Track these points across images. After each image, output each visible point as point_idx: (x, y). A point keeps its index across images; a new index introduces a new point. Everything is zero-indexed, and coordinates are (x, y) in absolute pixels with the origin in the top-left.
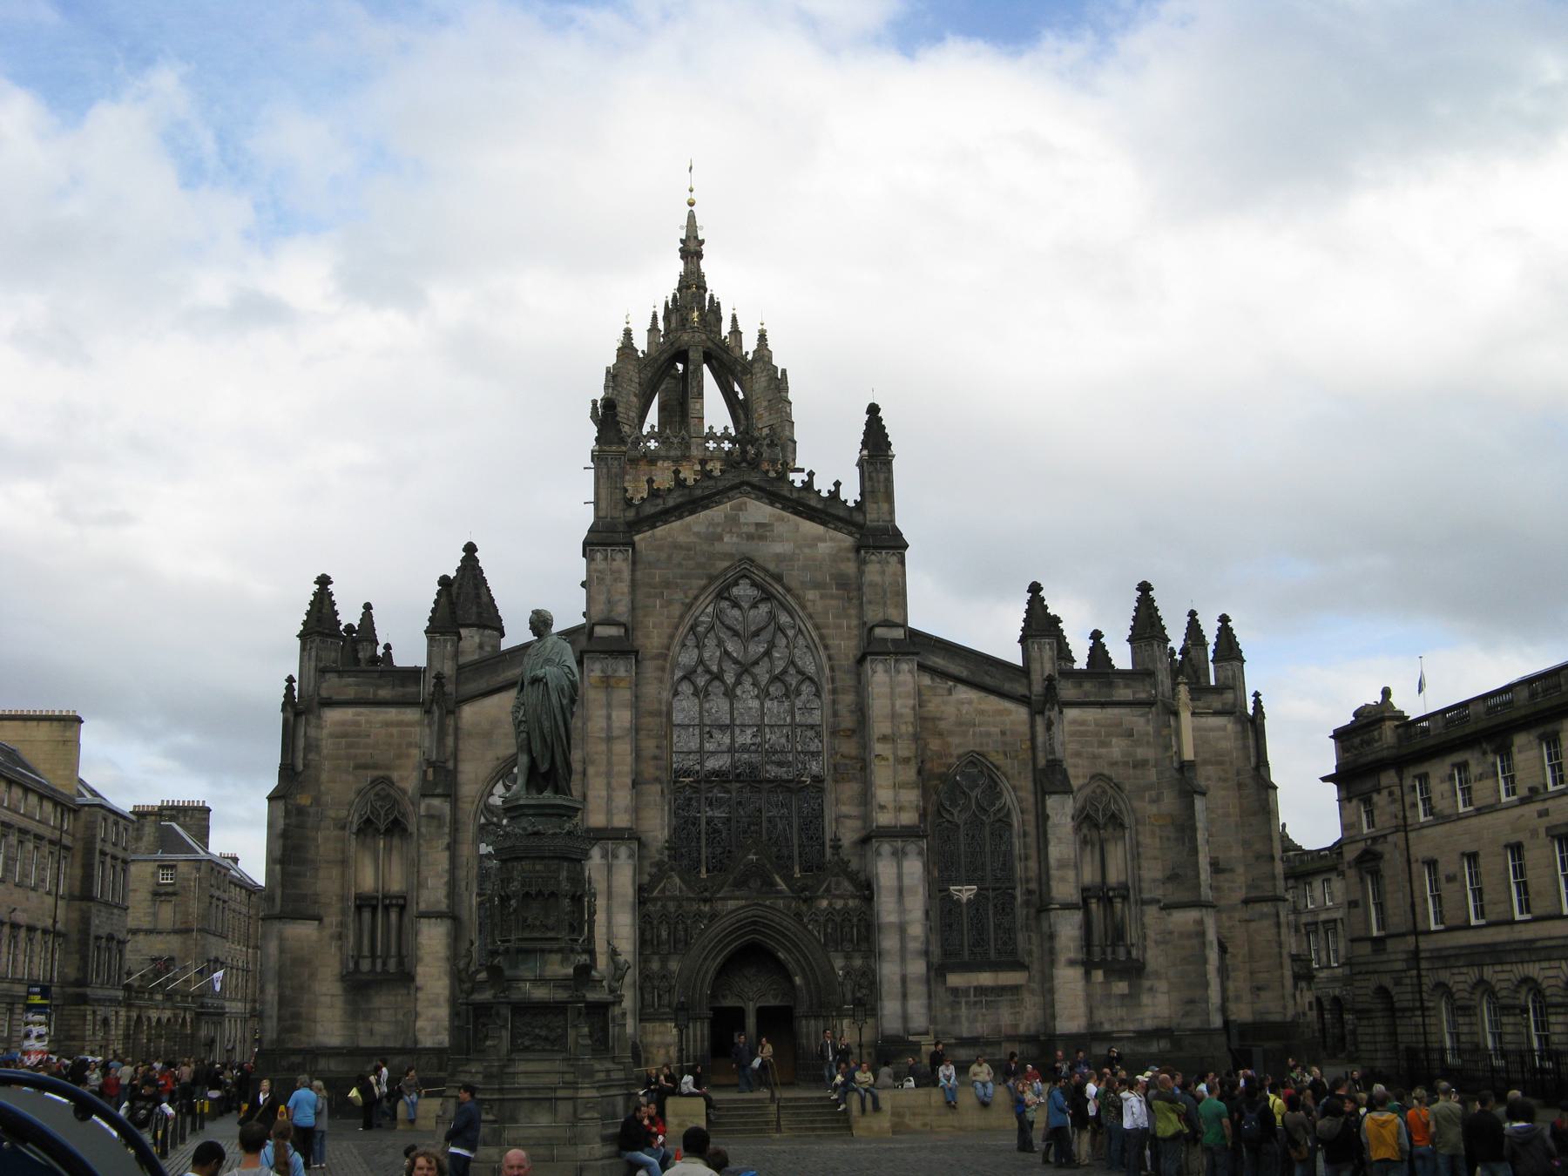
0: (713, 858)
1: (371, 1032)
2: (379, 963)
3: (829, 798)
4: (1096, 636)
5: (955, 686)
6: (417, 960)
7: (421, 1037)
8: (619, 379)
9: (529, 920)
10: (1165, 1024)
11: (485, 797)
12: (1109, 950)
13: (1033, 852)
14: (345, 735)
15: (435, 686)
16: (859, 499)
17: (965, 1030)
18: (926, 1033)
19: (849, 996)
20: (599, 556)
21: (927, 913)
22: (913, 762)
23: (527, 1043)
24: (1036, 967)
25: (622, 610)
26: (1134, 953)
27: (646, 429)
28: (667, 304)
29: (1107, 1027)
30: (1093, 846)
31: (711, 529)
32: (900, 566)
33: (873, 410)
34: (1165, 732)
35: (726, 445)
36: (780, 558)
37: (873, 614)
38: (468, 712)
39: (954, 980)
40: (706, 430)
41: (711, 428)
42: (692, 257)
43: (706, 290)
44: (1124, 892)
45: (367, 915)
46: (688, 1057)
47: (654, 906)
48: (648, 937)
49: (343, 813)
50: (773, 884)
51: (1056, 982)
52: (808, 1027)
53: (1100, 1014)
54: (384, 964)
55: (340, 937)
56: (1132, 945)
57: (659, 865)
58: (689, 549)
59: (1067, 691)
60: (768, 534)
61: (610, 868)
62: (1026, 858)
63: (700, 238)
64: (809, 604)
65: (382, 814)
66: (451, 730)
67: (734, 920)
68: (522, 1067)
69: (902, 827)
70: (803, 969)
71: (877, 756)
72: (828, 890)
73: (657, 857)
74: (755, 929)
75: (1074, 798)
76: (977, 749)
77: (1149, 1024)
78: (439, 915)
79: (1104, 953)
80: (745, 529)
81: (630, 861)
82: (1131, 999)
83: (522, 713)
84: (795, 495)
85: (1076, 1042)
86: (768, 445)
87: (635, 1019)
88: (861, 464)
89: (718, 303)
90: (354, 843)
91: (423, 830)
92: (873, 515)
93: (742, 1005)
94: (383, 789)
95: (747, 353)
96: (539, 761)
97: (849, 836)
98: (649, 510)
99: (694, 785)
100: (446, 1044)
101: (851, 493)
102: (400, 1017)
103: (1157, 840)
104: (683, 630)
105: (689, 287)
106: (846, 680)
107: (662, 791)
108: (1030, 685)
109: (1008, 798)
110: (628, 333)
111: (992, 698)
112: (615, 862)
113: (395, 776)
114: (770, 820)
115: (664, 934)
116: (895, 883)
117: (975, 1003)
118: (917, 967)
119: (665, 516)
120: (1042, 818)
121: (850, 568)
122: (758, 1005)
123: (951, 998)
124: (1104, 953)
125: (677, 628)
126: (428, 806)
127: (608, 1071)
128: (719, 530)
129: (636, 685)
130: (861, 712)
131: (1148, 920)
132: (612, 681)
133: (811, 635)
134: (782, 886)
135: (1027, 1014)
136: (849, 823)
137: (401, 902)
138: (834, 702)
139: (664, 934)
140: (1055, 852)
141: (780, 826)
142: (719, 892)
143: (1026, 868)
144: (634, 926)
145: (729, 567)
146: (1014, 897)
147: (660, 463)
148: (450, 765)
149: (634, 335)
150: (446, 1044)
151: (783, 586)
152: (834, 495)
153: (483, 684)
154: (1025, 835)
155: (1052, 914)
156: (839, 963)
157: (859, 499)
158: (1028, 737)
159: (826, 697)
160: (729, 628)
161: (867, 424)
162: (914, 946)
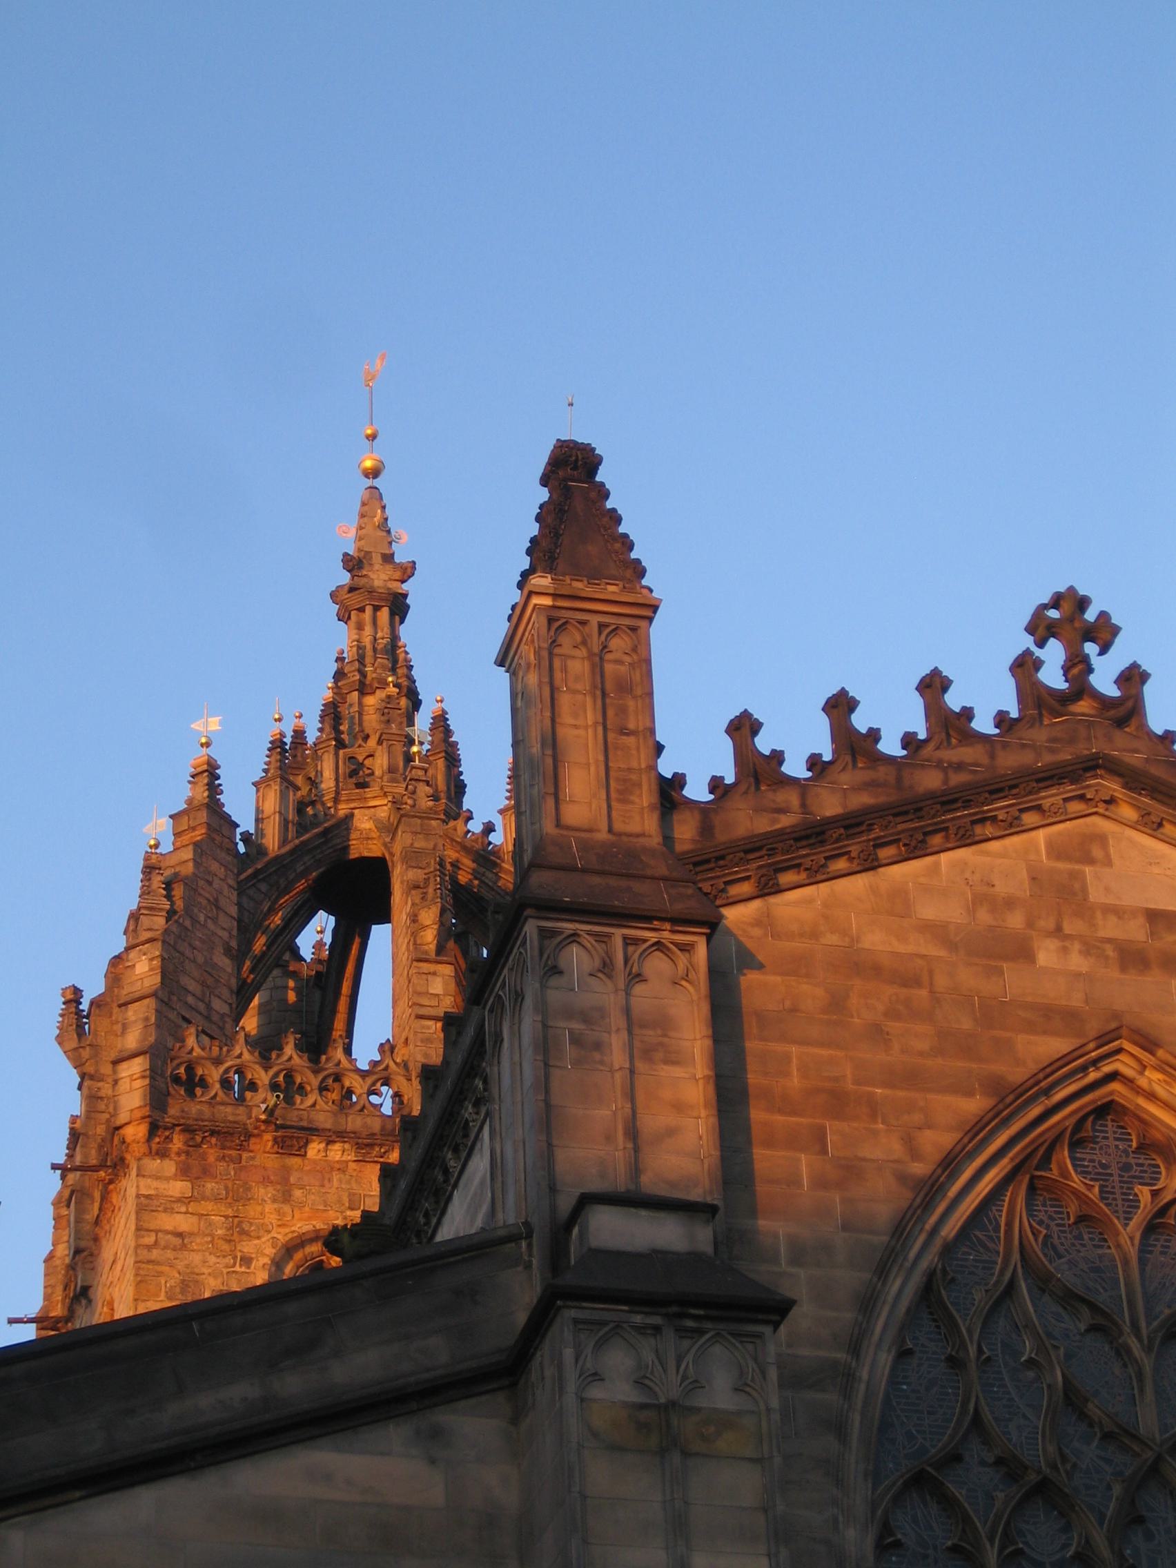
20: (577, 959)
31: (984, 916)
42: (376, 608)
58: (911, 981)
80: (1110, 928)
125: (882, 1271)
128: (1015, 921)
145: (1066, 1059)
147: (315, 1149)
149: (226, 779)
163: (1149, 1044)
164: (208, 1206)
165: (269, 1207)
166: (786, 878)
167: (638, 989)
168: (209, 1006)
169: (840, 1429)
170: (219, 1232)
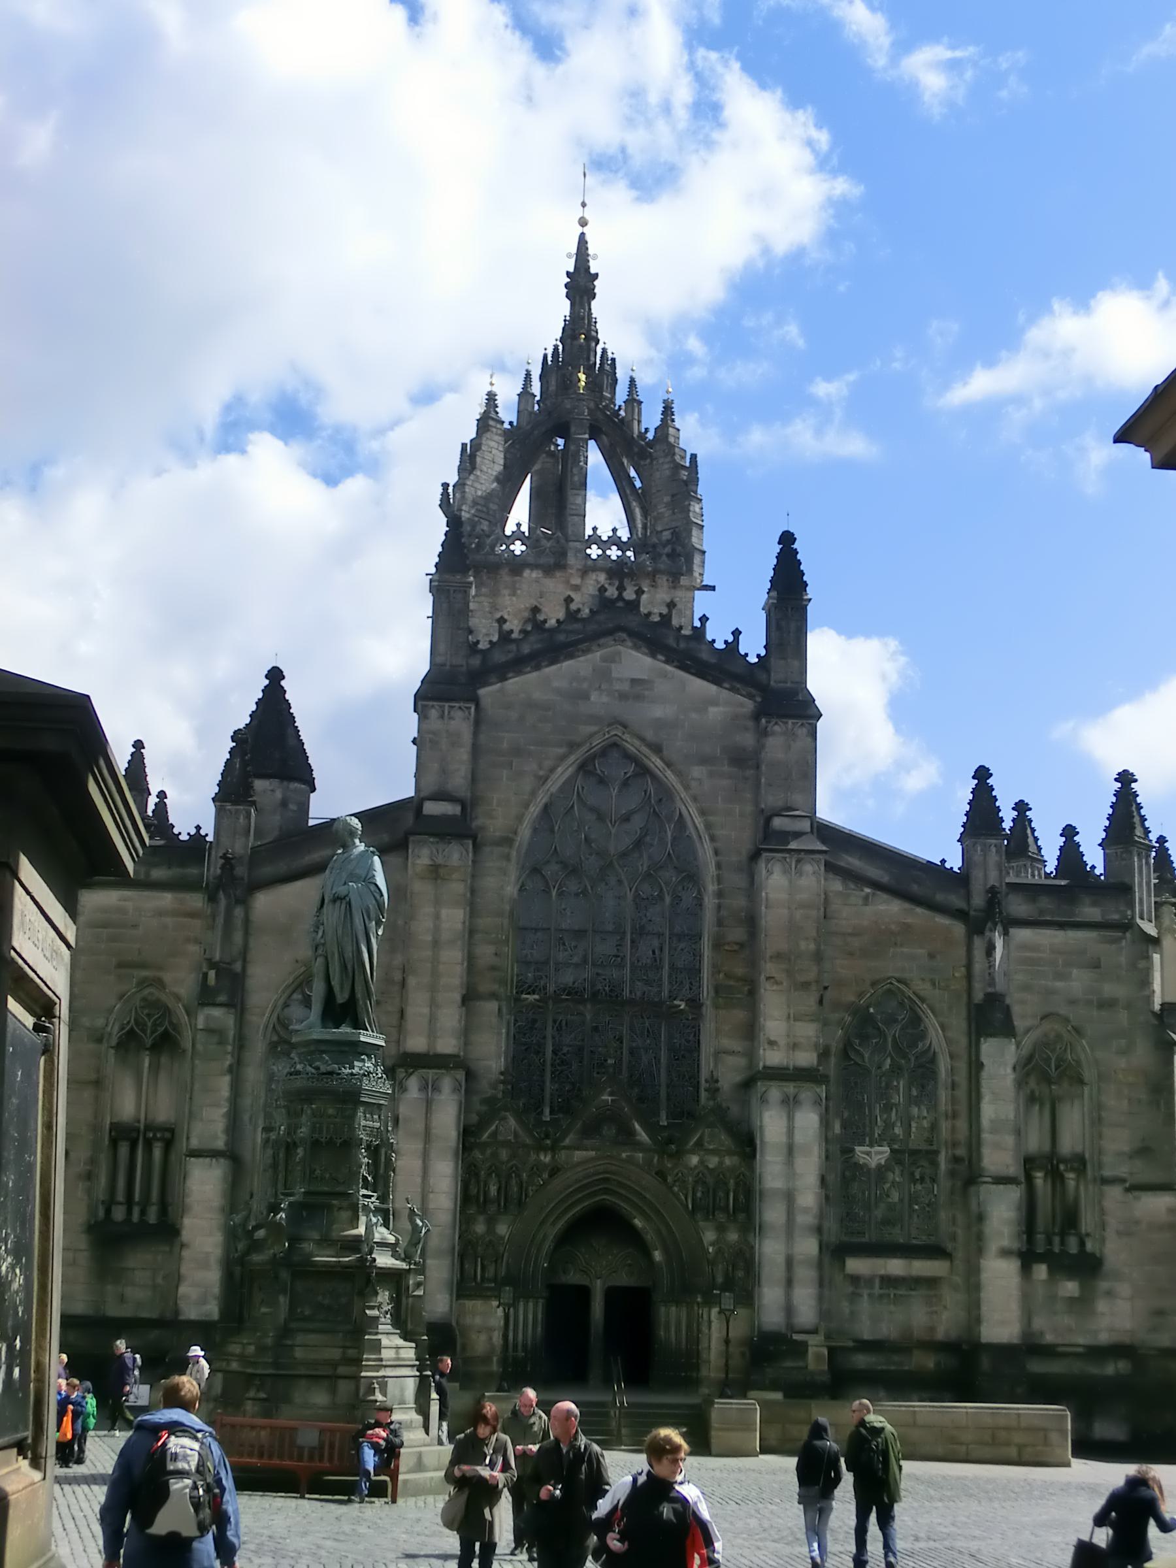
0: (559, 1096)
1: (122, 1299)
2: (136, 1211)
3: (708, 1027)
4: (1069, 832)
5: (874, 894)
6: (183, 1210)
7: (182, 1305)
8: (478, 460)
9: (318, 1172)
10: (1127, 1340)
11: (279, 1009)
12: (1057, 1240)
13: (963, 1108)
14: (105, 925)
15: (223, 867)
16: (763, 653)
17: (866, 1330)
18: (814, 1331)
20: (434, 713)
21: (823, 1180)
22: (814, 987)
23: (307, 1313)
24: (959, 1255)
25: (458, 781)
26: (1089, 1246)
27: (510, 529)
28: (545, 357)
29: (1049, 1338)
30: (1042, 1105)
32: (809, 739)
33: (787, 539)
34: (1142, 964)
35: (614, 553)
36: (659, 724)
37: (771, 799)
38: (264, 902)
39: (856, 1265)
40: (589, 532)
41: (595, 529)
42: (581, 297)
43: (597, 342)
44: (1079, 1163)
45: (124, 1149)
46: (515, 1346)
47: (483, 1153)
48: (473, 1191)
49: (100, 1022)
50: (631, 1133)
51: (985, 1276)
53: (1039, 1323)
54: (143, 1212)
55: (89, 1176)
56: (1088, 1235)
57: (490, 1101)
59: (1018, 907)
60: (646, 693)
61: (429, 1103)
62: (955, 1116)
63: (593, 271)
64: (694, 784)
65: (149, 1024)
66: (238, 922)
68: (300, 1339)
69: (796, 1068)
71: (768, 978)
72: (699, 1144)
73: (490, 1093)
75: (1018, 1045)
76: (897, 975)
77: (1104, 1338)
78: (214, 1154)
79: (1049, 1242)
80: (617, 686)
81: (455, 1097)
82: (1082, 1304)
83: (320, 934)
84: (682, 645)
85: (1004, 1351)
86: (668, 555)
87: (451, 1295)
88: (770, 610)
89: (613, 360)
90: (112, 1059)
91: (199, 1047)
92: (777, 677)
93: (586, 1283)
94: (151, 994)
95: (647, 430)
96: (337, 989)
97: (729, 1073)
98: (499, 657)
99: (541, 1004)
100: (216, 1316)
101: (753, 646)
102: (159, 1280)
103: (1126, 1101)
104: (534, 810)
105: (575, 337)
106: (738, 880)
107: (500, 1010)
108: (968, 897)
109: (935, 1036)
110: (491, 398)
111: (919, 910)
112: (436, 1097)
113: (167, 977)
114: (632, 1052)
116: (784, 1139)
117: (881, 1296)
118: (808, 1247)
119: (519, 664)
120: (976, 1066)
121: (747, 739)
123: (850, 1289)
124: (1049, 1242)
125: (527, 806)
126: (208, 1018)
127: (398, 1348)
128: (585, 685)
129: (473, 876)
130: (751, 921)
131: (1108, 1204)
132: (442, 871)
133: (694, 822)
134: (643, 1136)
135: (945, 1316)
136: (731, 1060)
137: (168, 1135)
138: (719, 907)
139: (493, 1190)
140: (988, 1111)
141: (645, 1059)
142: (563, 1138)
143: (954, 1129)
144: (456, 1178)
145: (595, 733)
146: (934, 1164)
147: (527, 573)
148: (238, 966)
149: (500, 401)
150: (216, 1316)
151: (662, 759)
152: (732, 647)
153: (282, 867)
154: (954, 1086)
155: (983, 1188)
156: (709, 1236)
157: (763, 653)
158: (964, 962)
159: (709, 902)
160: (592, 809)
161: (779, 557)
162: (805, 1219)
163: (625, 727)
164: (482, 598)
165: (507, 598)
166: (510, 675)
167: (453, 722)
168: (488, 508)
169: (507, 858)
170: (487, 609)
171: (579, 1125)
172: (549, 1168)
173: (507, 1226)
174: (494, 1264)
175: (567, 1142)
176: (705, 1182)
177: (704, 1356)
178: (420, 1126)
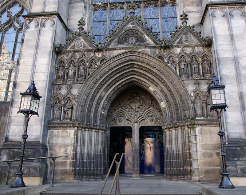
19: (199, 111)
46: (82, 154)
47: (67, 56)
50: (143, 41)
52: (170, 136)
67: (117, 63)
70: (166, 96)
74: (133, 71)
87: (41, 125)
107: (85, 7)
112: (43, 29)
115: (71, 73)
116: (227, 33)
122: (141, 125)
134: (149, 41)
139: (71, 73)
156: (191, 88)
171: (116, 39)
172: (101, 59)
173: (78, 90)
174: (70, 110)
175: (110, 47)
176: (185, 61)
177: (194, 156)
178: (34, 43)
